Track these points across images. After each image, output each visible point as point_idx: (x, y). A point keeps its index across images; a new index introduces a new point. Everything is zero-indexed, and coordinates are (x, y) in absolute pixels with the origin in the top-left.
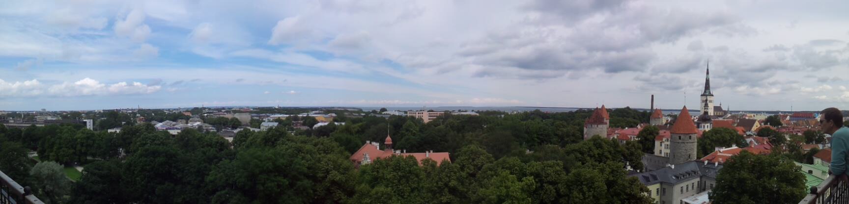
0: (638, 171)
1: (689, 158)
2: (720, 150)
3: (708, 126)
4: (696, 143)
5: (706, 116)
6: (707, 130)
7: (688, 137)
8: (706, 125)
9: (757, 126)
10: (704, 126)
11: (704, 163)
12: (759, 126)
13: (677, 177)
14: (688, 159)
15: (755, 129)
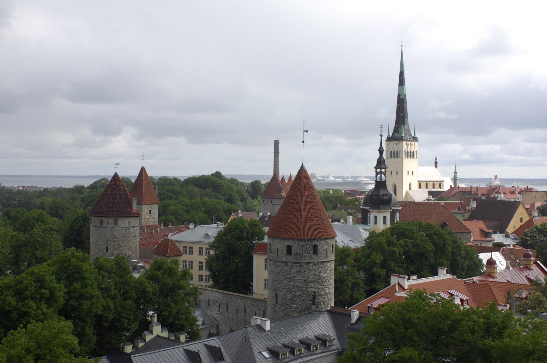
0: (183, 338)
1: (314, 304)
2: (401, 281)
3: (385, 217)
4: (333, 265)
5: (382, 192)
6: (381, 227)
7: (309, 247)
8: (380, 217)
9: (521, 220)
10: (376, 217)
11: (349, 316)
12: (526, 218)
13: (274, 354)
14: (309, 308)
15: (517, 227)
